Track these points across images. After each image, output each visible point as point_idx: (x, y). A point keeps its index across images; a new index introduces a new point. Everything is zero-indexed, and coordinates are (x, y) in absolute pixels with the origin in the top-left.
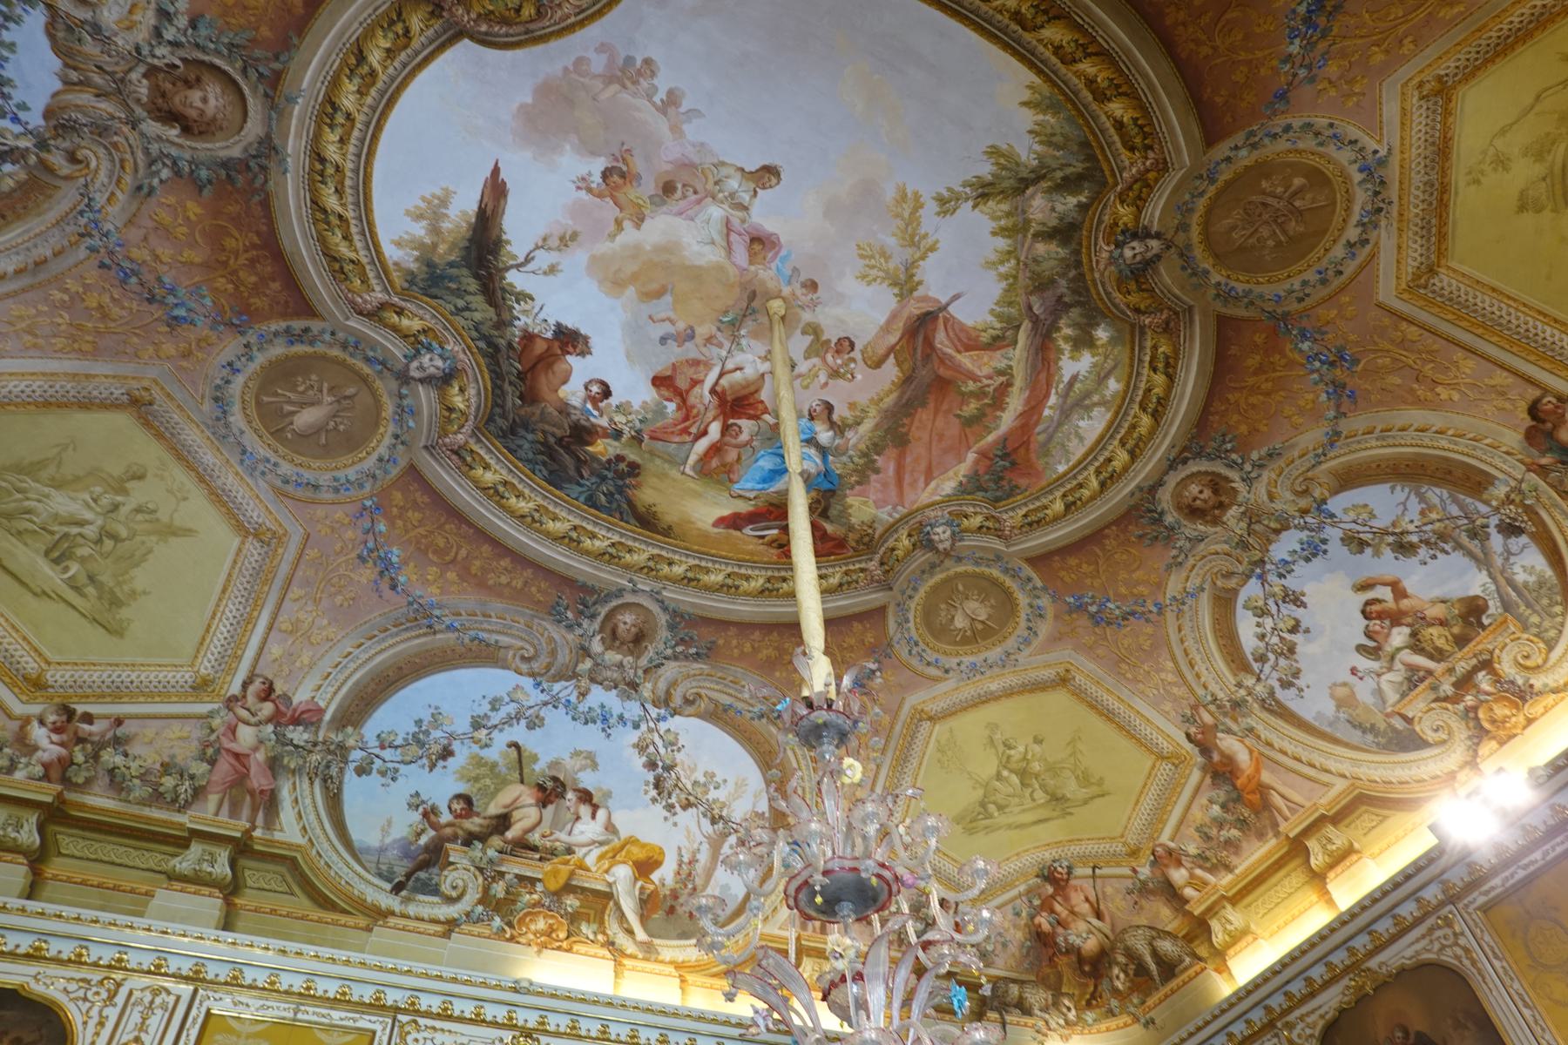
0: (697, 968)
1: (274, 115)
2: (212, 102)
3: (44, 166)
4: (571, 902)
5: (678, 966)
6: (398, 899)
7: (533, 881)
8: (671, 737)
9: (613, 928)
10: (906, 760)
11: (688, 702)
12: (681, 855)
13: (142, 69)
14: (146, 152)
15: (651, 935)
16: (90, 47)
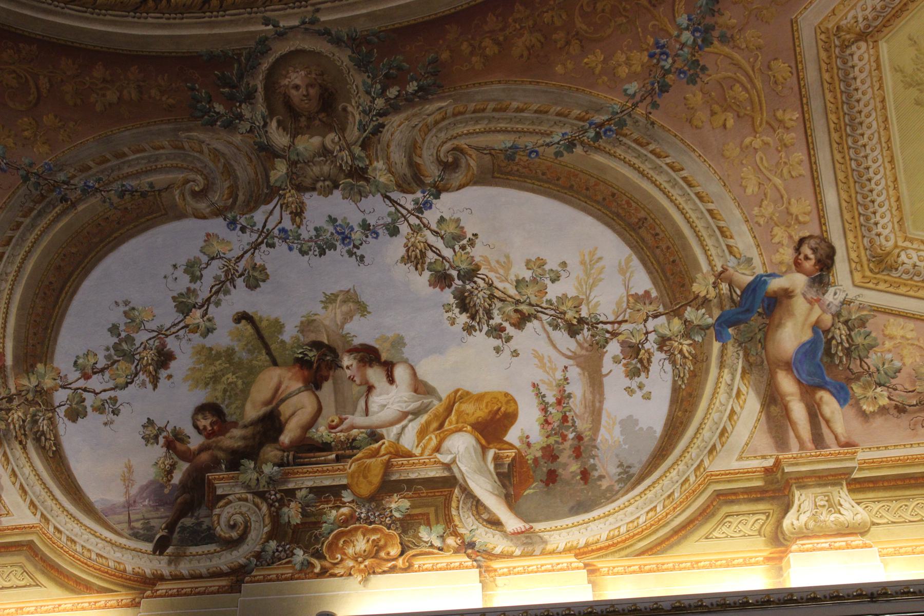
0: (613, 546)
4: (398, 505)
5: (580, 552)
6: (164, 559)
7: (335, 491)
8: (451, 229)
9: (467, 523)
10: (854, 124)
11: (449, 167)
12: (541, 396)
15: (526, 521)
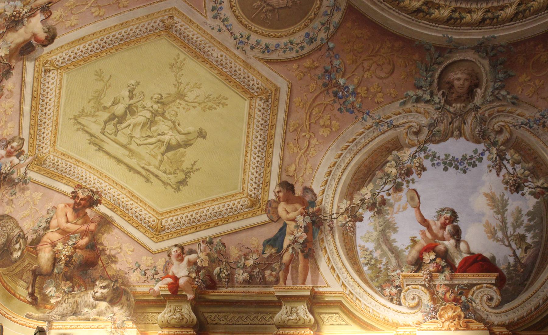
1: (461, 47)
2: (459, 76)
3: (505, 143)
13: (448, 107)
14: (492, 101)
16: (441, 127)
